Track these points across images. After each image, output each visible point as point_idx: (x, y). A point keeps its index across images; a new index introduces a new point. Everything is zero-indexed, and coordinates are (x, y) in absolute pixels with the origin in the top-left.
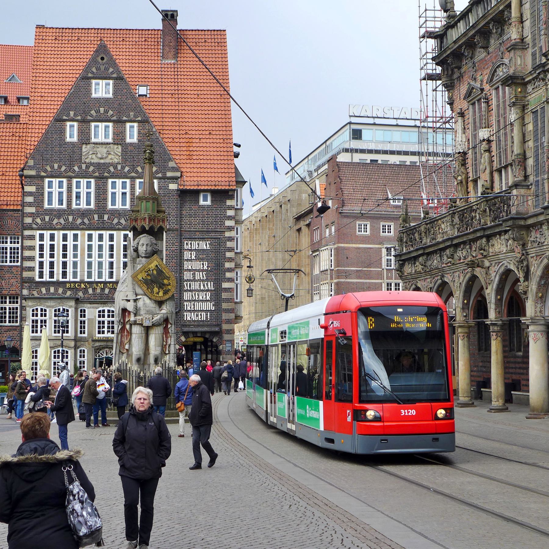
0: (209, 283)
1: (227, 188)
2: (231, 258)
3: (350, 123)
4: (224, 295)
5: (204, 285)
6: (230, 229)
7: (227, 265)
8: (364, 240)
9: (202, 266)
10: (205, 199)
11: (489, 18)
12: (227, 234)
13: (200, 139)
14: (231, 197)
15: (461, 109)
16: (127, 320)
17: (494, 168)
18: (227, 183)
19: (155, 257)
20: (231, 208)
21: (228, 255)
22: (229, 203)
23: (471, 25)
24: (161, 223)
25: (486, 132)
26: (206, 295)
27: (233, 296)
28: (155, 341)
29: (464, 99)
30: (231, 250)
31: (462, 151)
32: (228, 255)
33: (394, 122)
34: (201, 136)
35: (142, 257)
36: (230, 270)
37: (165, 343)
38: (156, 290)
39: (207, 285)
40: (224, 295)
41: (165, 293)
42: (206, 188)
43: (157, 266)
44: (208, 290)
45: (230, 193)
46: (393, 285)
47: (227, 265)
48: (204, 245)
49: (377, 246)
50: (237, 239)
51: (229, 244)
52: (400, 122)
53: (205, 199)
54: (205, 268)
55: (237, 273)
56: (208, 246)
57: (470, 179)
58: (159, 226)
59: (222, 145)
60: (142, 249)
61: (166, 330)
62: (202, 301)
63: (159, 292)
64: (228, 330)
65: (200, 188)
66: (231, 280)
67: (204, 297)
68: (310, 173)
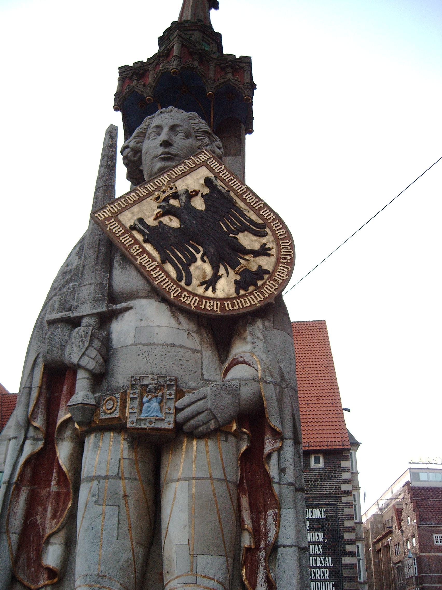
0: (327, 558)
1: (341, 447)
2: (350, 527)
3: (410, 469)
4: (346, 573)
5: (321, 561)
6: (347, 493)
7: (347, 536)
9: (317, 538)
10: (317, 462)
12: (344, 500)
13: (308, 404)
14: (346, 458)
18: (341, 443)
19: (201, 156)
20: (346, 470)
21: (347, 524)
22: (344, 464)
24: (229, 76)
26: (323, 573)
30: (350, 518)
32: (347, 524)
34: (309, 402)
36: (352, 542)
37: (247, 541)
39: (324, 561)
40: (346, 573)
41: (248, 280)
42: (318, 448)
43: (208, 182)
44: (325, 567)
47: (347, 536)
48: (318, 513)
50: (355, 507)
51: (347, 511)
53: (317, 462)
54: (321, 539)
55: (358, 546)
56: (323, 514)
58: (221, 81)
59: (332, 408)
61: (252, 462)
62: (320, 580)
63: (216, 278)
65: (311, 448)
66: (352, 554)
67: (322, 575)
68: (381, 509)
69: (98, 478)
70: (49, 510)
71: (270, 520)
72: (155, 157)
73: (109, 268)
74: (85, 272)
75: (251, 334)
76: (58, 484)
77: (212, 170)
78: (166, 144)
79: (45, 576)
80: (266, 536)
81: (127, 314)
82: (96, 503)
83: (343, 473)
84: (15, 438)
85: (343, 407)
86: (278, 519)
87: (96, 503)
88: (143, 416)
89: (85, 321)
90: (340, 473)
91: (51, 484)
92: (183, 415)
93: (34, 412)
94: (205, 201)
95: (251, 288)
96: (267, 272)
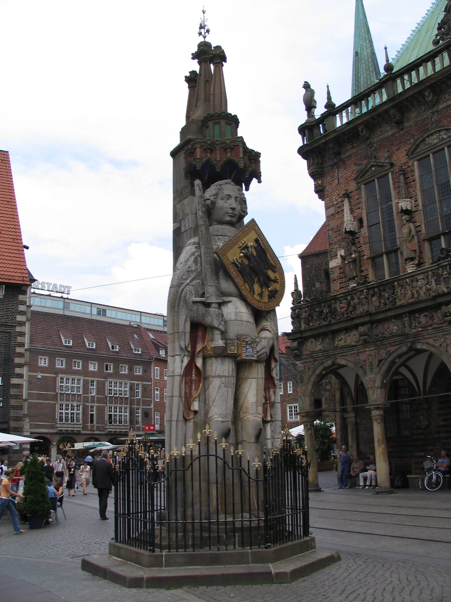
1: (21, 282)
2: (21, 353)
4: (13, 391)
7: (17, 360)
8: (43, 370)
11: (428, 84)
12: (18, 329)
15: (346, 190)
16: (199, 347)
17: (422, 237)
18: (21, 279)
20: (23, 303)
21: (19, 350)
22: (21, 297)
23: (370, 107)
25: (409, 203)
27: (22, 392)
28: (257, 395)
29: (355, 179)
31: (352, 230)
32: (19, 350)
33: (47, 293)
35: (221, 222)
36: (21, 366)
38: (256, 287)
40: (13, 391)
45: (23, 288)
46: (64, 406)
47: (17, 360)
49: (53, 375)
51: (19, 339)
52: (53, 294)
57: (365, 257)
60: (226, 205)
61: (268, 371)
63: (262, 292)
64: (15, 428)
66: (21, 376)
69: (225, 376)
70: (194, 387)
71: (272, 393)
72: (227, 213)
73: (218, 278)
74: (207, 278)
75: (270, 318)
76: (196, 376)
77: (256, 233)
78: (233, 209)
79: (193, 414)
80: (270, 399)
81: (229, 304)
82: (225, 386)
83: (20, 306)
84: (179, 355)
85: (24, 244)
86: (275, 393)
87: (225, 386)
88: (247, 354)
89: (214, 305)
90: (17, 305)
91: (192, 376)
92: (259, 354)
93: (188, 344)
94: (256, 251)
95: (273, 299)
96: (278, 291)
